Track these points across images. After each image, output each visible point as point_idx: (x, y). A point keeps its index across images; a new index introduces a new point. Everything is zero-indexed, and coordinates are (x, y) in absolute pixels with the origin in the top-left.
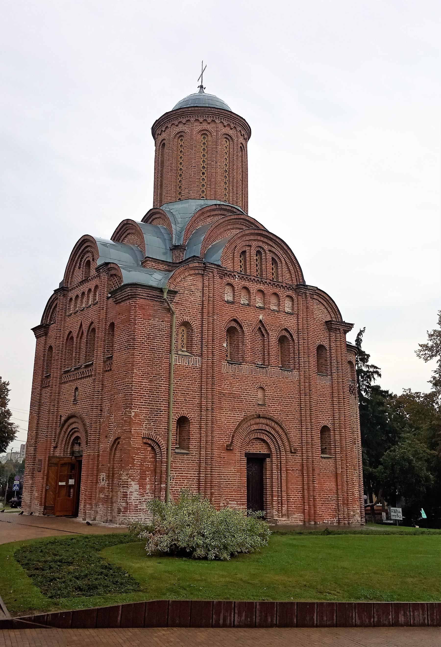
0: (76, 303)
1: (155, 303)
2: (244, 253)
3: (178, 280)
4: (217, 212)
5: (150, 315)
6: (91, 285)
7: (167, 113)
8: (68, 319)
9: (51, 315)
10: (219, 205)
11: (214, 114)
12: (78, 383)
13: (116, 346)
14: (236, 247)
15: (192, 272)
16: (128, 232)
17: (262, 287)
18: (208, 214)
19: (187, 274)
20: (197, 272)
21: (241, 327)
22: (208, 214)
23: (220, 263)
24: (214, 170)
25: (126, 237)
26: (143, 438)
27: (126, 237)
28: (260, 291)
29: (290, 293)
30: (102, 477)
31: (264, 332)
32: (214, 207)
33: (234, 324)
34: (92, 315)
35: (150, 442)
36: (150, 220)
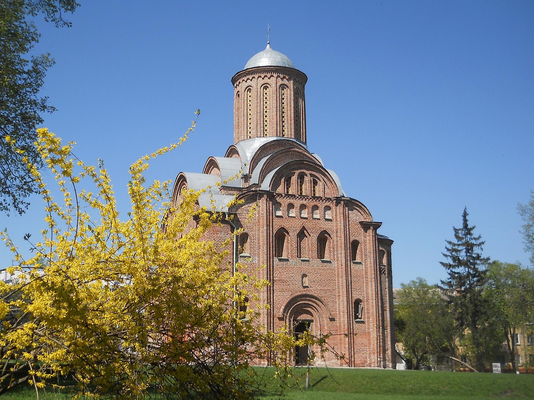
17: (304, 202)
29: (328, 204)
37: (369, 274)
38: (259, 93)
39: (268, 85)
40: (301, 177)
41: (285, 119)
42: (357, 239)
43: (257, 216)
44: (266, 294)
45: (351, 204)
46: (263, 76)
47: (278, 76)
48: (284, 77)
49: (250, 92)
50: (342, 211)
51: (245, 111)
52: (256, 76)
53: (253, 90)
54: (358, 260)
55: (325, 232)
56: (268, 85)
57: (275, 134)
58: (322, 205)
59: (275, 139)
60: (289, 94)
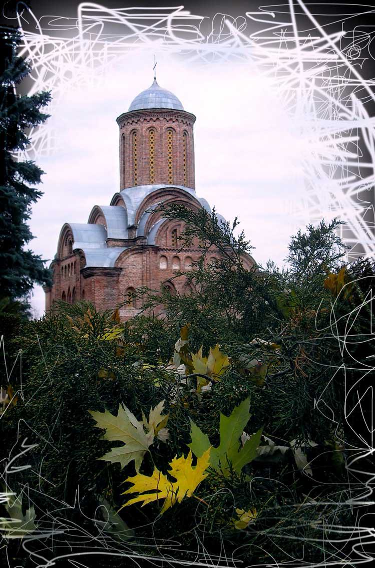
0: (66, 270)
1: (108, 278)
2: (175, 230)
3: (123, 260)
4: (163, 194)
7: (124, 114)
10: (164, 189)
11: (158, 113)
14: (168, 228)
15: (132, 253)
17: (190, 254)
18: (156, 197)
19: (130, 254)
20: (137, 251)
21: (174, 286)
22: (156, 197)
24: (160, 160)
25: (98, 217)
27: (98, 217)
28: (188, 257)
31: (192, 287)
32: (160, 191)
33: (168, 284)
46: (148, 119)
48: (171, 119)
49: (136, 135)
53: (139, 134)
60: (177, 137)
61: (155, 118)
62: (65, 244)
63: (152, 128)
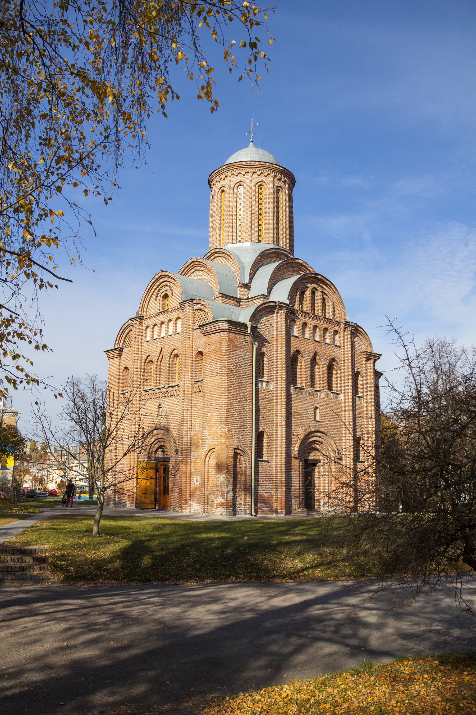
1: (240, 336)
5: (237, 347)
6: (173, 316)
8: (145, 345)
9: (124, 340)
12: (162, 401)
13: (208, 372)
16: (196, 268)
17: (316, 323)
23: (288, 302)
26: (235, 449)
29: (336, 328)
30: (195, 479)
34: (174, 343)
35: (239, 452)
36: (212, 258)
37: (369, 410)
38: (254, 192)
39: (263, 184)
40: (313, 293)
41: (263, 228)
42: (359, 370)
43: (275, 333)
44: (284, 429)
45: (356, 331)
46: (259, 172)
47: (275, 176)
50: (349, 338)
51: (235, 210)
52: (251, 172)
54: (360, 395)
55: (333, 359)
56: (263, 184)
57: (271, 241)
58: (332, 328)
59: (272, 246)
61: (266, 173)
62: (154, 296)
63: (261, 183)
